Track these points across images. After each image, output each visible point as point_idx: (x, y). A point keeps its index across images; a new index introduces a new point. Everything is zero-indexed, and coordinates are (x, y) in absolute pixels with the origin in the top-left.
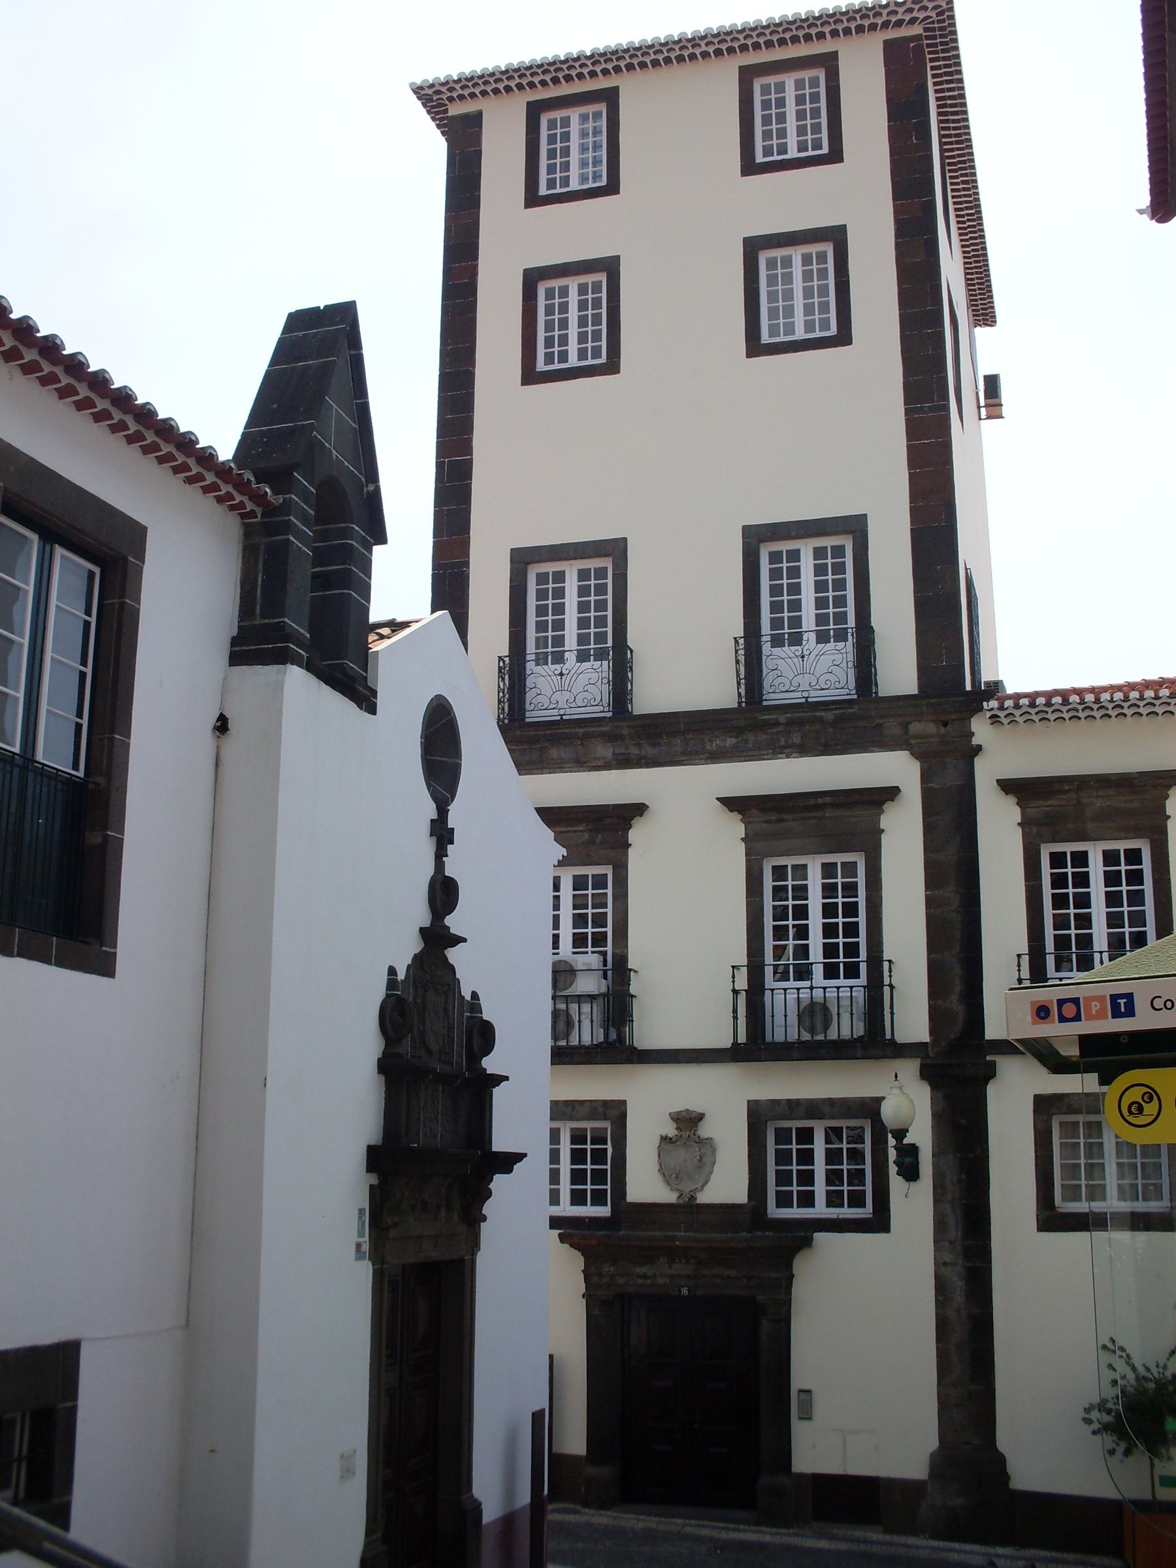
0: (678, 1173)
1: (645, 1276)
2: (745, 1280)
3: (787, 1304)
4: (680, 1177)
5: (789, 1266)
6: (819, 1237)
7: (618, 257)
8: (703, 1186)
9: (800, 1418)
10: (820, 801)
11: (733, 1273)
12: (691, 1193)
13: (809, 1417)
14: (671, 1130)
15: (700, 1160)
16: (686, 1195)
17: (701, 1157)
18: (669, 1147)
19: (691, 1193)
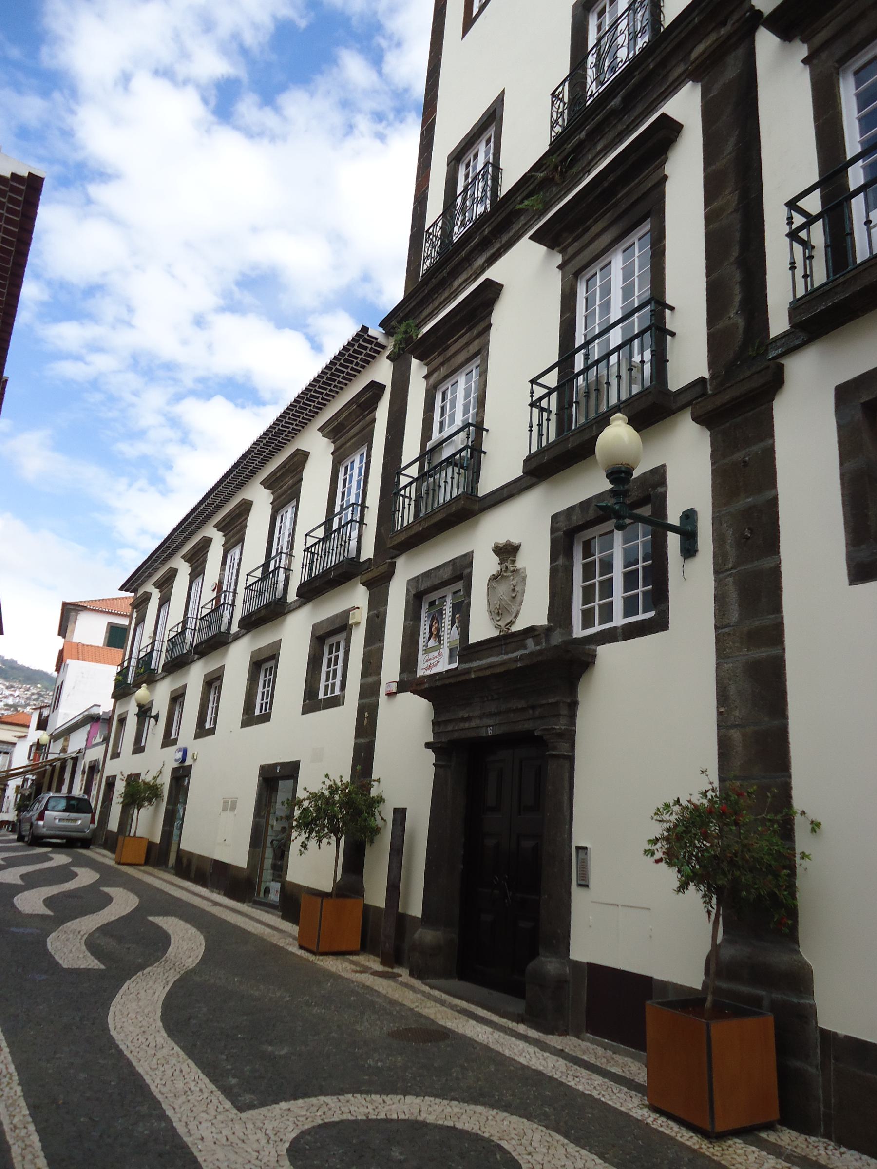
1: (464, 720)
2: (531, 712)
3: (569, 736)
5: (573, 689)
6: (604, 652)
8: (516, 617)
9: (579, 885)
10: (606, 184)
11: (522, 704)
13: (586, 883)
15: (514, 590)
18: (494, 584)
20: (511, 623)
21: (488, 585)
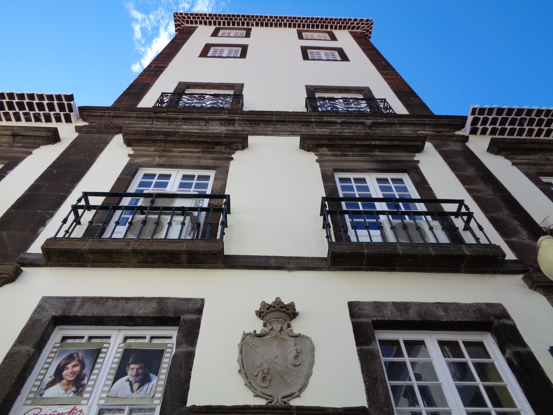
0: (266, 371)
4: (269, 377)
7: (248, 45)
8: (301, 390)
12: (285, 400)
14: (258, 326)
15: (297, 357)
16: (277, 401)
17: (298, 353)
19: (285, 400)
20: (291, 396)
21: (243, 340)
